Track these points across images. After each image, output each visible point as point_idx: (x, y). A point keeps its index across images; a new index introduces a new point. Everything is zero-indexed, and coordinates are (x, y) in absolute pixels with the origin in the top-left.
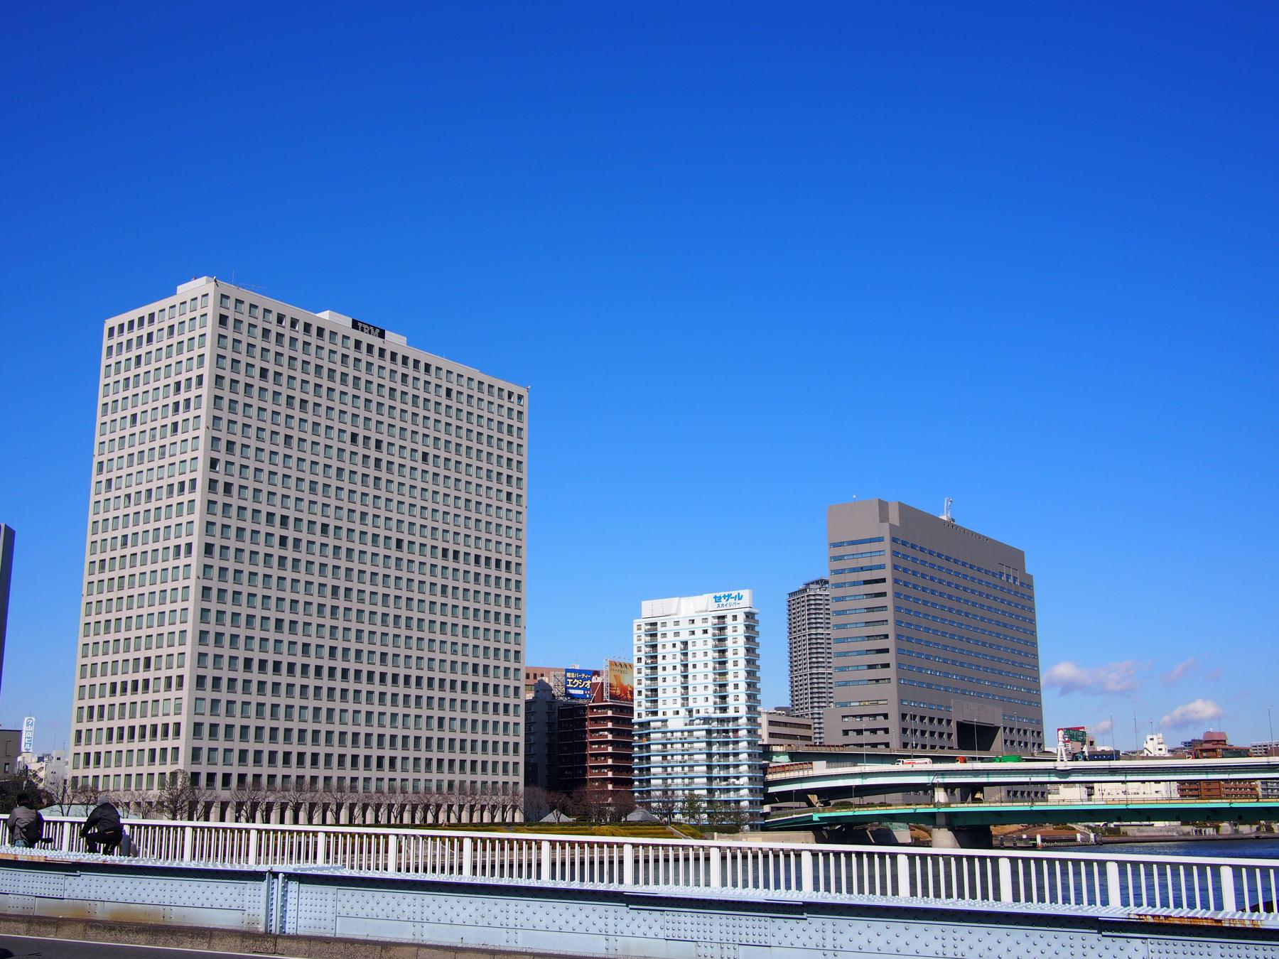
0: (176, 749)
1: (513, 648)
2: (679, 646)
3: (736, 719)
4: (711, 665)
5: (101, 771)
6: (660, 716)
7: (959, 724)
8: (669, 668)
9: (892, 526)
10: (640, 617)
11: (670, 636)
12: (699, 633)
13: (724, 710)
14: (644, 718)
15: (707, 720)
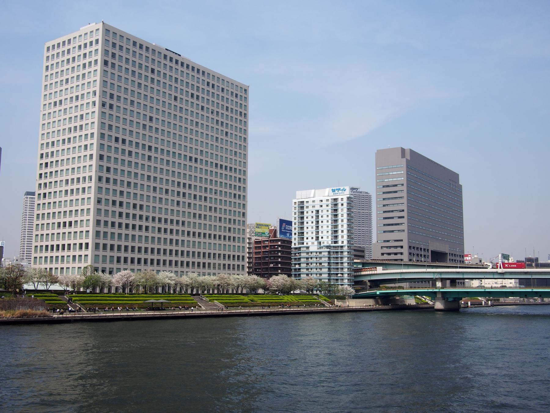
0: (86, 256)
1: (242, 211)
2: (314, 212)
3: (342, 247)
4: (330, 221)
5: (54, 266)
6: (305, 245)
7: (432, 251)
8: (310, 223)
9: (407, 160)
10: (295, 199)
11: (310, 208)
14: (297, 246)
15: (328, 247)
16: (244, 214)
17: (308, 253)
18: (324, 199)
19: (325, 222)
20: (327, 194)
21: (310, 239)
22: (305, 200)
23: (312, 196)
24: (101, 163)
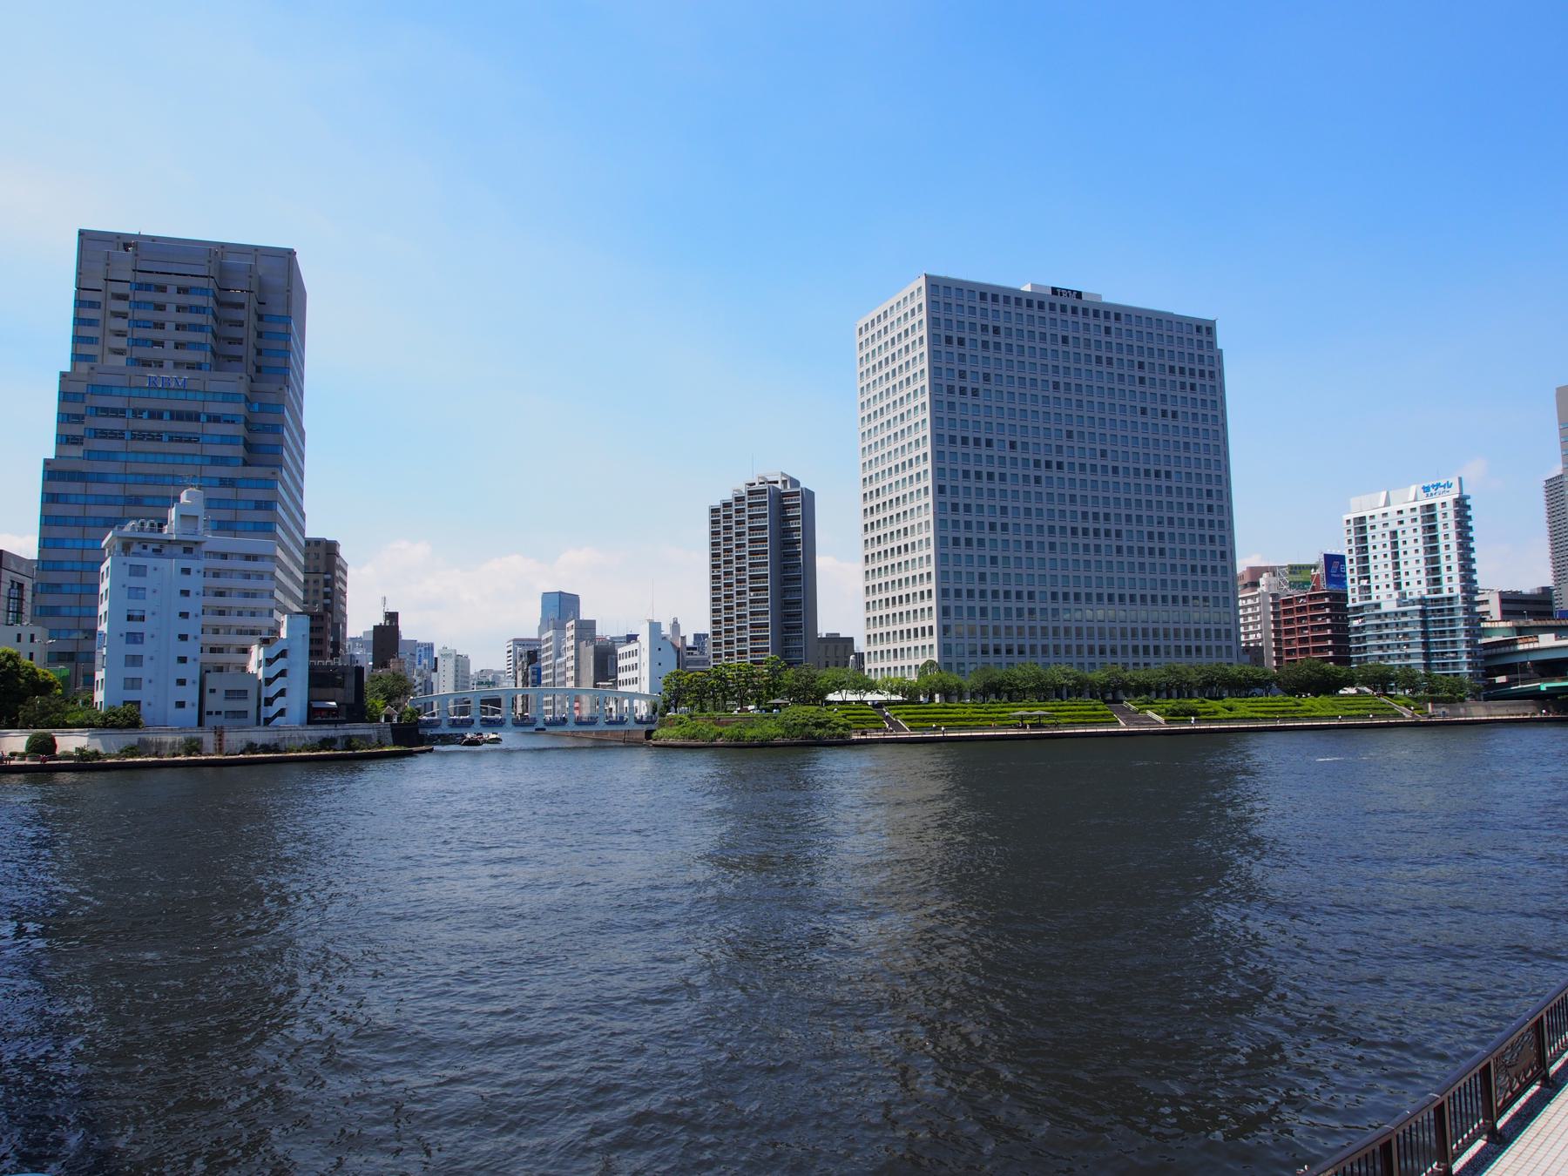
1: (1218, 548)
3: (1450, 599)
8: (1380, 557)
11: (1379, 528)
12: (1407, 522)
13: (1439, 591)
14: (1358, 603)
15: (1422, 601)
16: (1223, 554)
17: (1378, 616)
18: (1406, 507)
19: (1411, 552)
20: (1412, 498)
21: (1383, 587)
22: (1367, 514)
23: (1382, 503)
24: (942, 499)
